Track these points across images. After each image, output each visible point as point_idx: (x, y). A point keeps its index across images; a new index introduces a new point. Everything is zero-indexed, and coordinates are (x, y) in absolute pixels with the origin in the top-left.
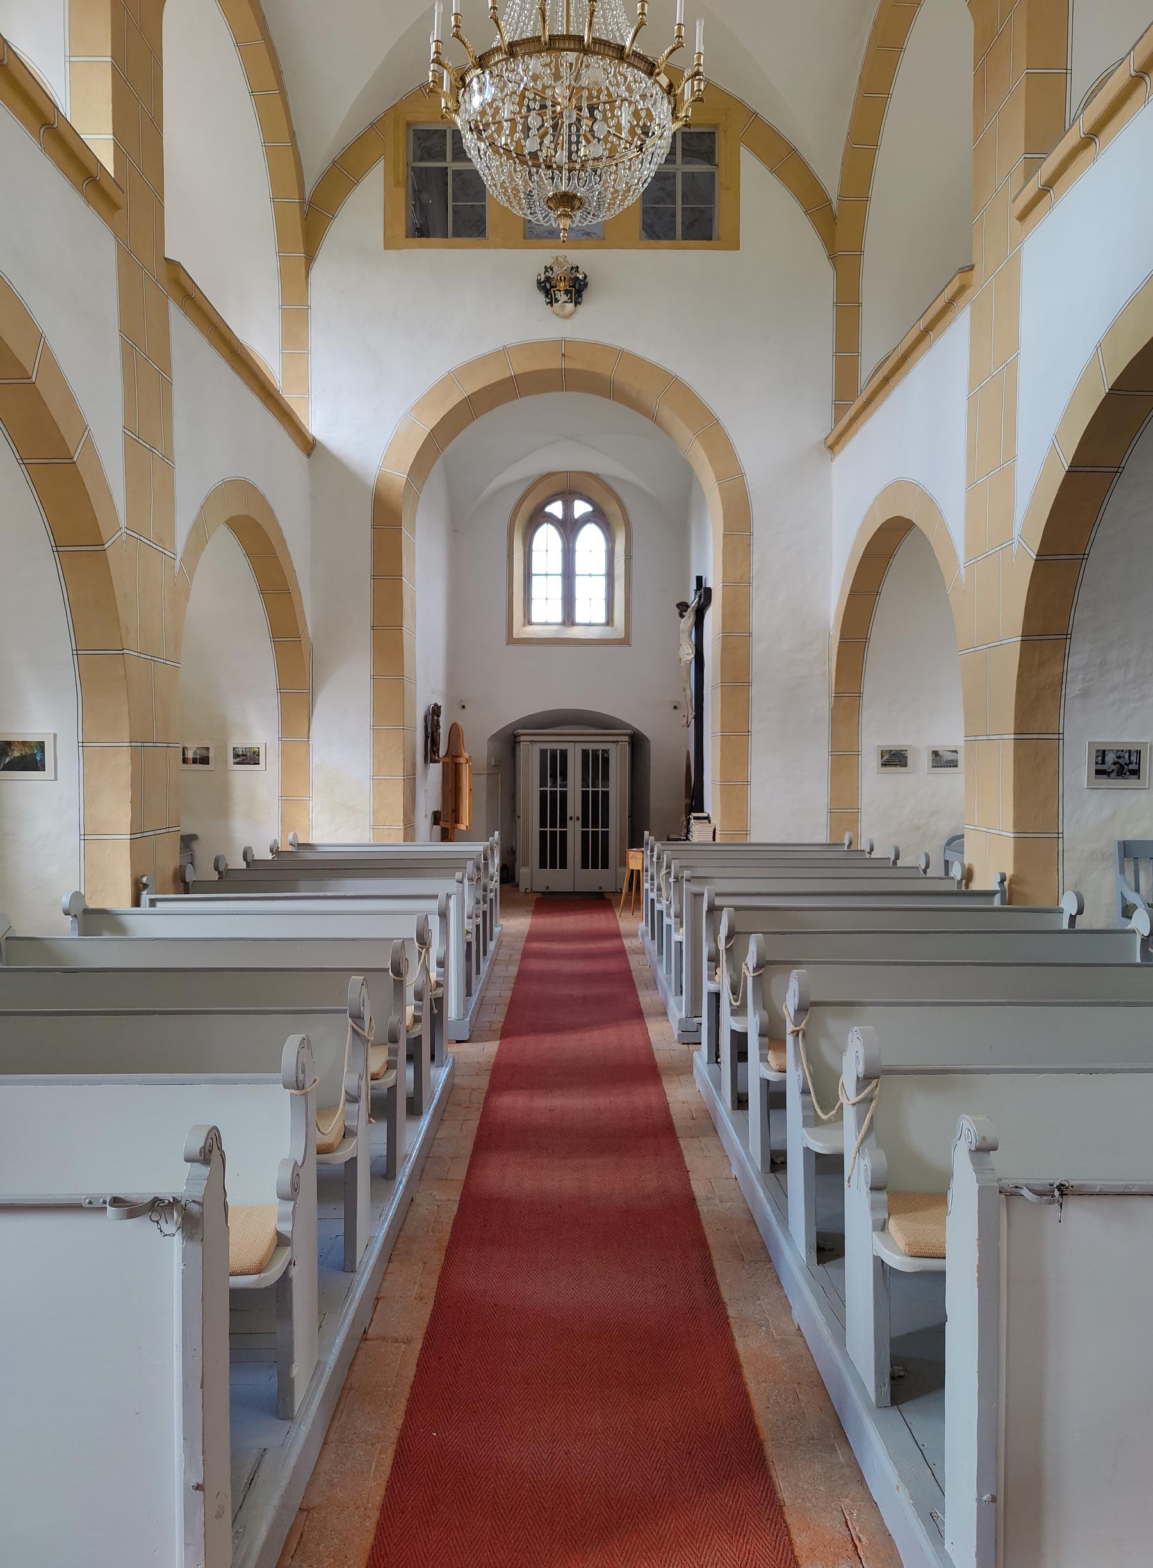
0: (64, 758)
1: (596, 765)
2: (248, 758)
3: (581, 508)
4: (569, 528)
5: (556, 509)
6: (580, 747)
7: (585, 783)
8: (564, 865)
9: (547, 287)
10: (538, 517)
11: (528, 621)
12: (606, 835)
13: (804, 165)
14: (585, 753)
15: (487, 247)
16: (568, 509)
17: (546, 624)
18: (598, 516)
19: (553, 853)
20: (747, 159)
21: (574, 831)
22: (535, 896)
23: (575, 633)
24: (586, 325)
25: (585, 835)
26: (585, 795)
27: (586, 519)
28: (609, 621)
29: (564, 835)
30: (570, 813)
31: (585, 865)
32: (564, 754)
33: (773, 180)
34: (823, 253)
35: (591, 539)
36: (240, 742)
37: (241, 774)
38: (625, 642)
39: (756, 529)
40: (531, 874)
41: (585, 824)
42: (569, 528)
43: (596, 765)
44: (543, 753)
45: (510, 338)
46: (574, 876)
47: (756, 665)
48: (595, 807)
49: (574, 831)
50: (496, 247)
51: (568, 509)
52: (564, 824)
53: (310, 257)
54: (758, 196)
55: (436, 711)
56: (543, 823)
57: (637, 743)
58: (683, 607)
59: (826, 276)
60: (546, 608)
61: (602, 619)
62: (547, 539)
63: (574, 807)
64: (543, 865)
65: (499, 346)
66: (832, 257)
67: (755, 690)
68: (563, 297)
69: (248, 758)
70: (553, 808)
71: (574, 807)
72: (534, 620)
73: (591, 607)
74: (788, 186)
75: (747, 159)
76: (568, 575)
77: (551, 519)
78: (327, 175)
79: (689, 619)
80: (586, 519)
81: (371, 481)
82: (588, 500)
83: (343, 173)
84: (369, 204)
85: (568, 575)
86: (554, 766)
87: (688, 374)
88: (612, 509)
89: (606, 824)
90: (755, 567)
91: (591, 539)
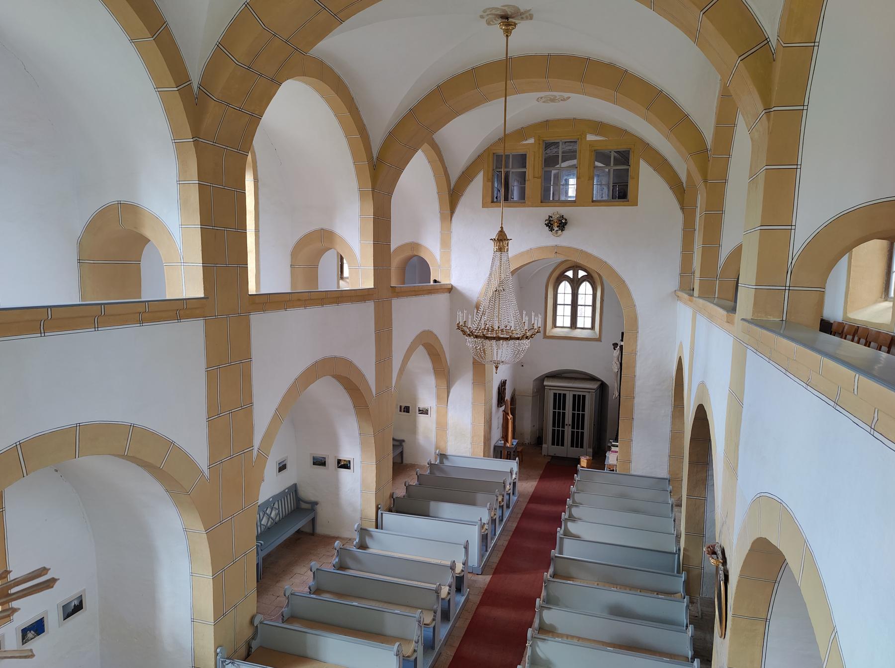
0: (356, 465)
1: (579, 401)
2: (424, 412)
3: (581, 273)
4: (575, 284)
5: (570, 274)
6: (572, 394)
7: (574, 409)
8: (563, 445)
9: (549, 225)
10: (561, 277)
11: (554, 325)
12: (582, 433)
13: (671, 167)
14: (574, 396)
15: (524, 206)
16: (576, 274)
17: (563, 327)
18: (589, 278)
19: (558, 439)
20: (643, 165)
21: (568, 431)
22: (548, 460)
23: (577, 333)
24: (565, 239)
25: (573, 432)
26: (573, 414)
27: (584, 279)
28: (593, 327)
29: (563, 432)
30: (566, 422)
31: (572, 446)
32: (565, 395)
33: (655, 173)
34: (678, 207)
35: (585, 289)
36: (422, 405)
37: (422, 418)
38: (599, 340)
39: (640, 330)
40: (548, 448)
41: (573, 428)
42: (575, 284)
43: (579, 401)
44: (555, 394)
45: (533, 245)
46: (566, 450)
47: (637, 390)
48: (578, 421)
49: (568, 431)
50: (528, 206)
51: (576, 274)
52: (563, 427)
53: (452, 212)
54: (647, 181)
55: (503, 384)
56: (554, 426)
57: (603, 387)
58: (615, 345)
59: (679, 216)
60: (563, 318)
61: (589, 326)
62: (565, 288)
63: (568, 419)
64: (553, 444)
65: (528, 248)
66: (682, 209)
67: (637, 400)
68: (556, 229)
69: (424, 412)
70: (559, 419)
71: (568, 419)
72: (558, 325)
73: (585, 319)
74: (662, 176)
75: (643, 165)
76: (574, 305)
77: (567, 278)
78: (460, 178)
79: (617, 352)
80: (584, 279)
81: (475, 303)
82: (585, 270)
83: (466, 177)
84: (477, 188)
85: (574, 305)
86: (560, 400)
87: (611, 262)
88: (595, 276)
89: (583, 428)
90: (638, 347)
91: (585, 289)
